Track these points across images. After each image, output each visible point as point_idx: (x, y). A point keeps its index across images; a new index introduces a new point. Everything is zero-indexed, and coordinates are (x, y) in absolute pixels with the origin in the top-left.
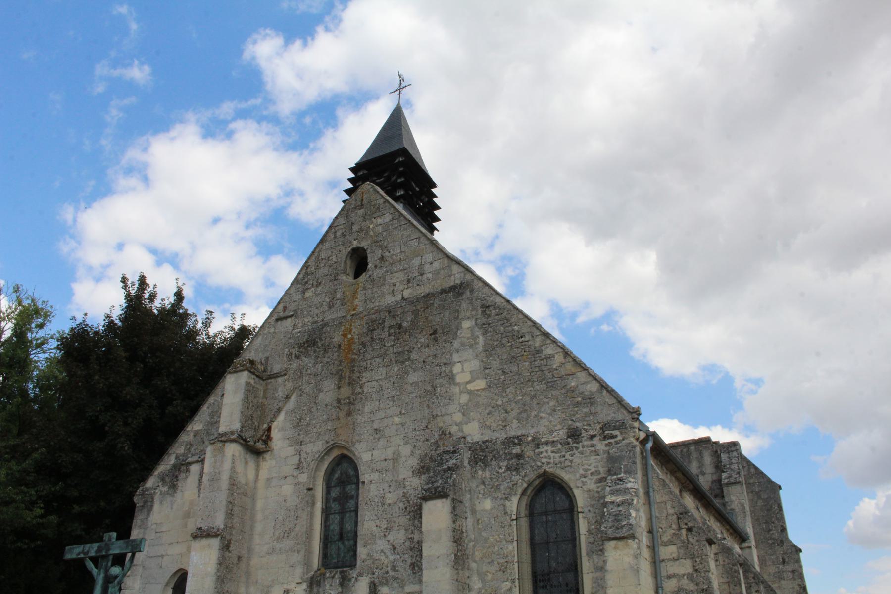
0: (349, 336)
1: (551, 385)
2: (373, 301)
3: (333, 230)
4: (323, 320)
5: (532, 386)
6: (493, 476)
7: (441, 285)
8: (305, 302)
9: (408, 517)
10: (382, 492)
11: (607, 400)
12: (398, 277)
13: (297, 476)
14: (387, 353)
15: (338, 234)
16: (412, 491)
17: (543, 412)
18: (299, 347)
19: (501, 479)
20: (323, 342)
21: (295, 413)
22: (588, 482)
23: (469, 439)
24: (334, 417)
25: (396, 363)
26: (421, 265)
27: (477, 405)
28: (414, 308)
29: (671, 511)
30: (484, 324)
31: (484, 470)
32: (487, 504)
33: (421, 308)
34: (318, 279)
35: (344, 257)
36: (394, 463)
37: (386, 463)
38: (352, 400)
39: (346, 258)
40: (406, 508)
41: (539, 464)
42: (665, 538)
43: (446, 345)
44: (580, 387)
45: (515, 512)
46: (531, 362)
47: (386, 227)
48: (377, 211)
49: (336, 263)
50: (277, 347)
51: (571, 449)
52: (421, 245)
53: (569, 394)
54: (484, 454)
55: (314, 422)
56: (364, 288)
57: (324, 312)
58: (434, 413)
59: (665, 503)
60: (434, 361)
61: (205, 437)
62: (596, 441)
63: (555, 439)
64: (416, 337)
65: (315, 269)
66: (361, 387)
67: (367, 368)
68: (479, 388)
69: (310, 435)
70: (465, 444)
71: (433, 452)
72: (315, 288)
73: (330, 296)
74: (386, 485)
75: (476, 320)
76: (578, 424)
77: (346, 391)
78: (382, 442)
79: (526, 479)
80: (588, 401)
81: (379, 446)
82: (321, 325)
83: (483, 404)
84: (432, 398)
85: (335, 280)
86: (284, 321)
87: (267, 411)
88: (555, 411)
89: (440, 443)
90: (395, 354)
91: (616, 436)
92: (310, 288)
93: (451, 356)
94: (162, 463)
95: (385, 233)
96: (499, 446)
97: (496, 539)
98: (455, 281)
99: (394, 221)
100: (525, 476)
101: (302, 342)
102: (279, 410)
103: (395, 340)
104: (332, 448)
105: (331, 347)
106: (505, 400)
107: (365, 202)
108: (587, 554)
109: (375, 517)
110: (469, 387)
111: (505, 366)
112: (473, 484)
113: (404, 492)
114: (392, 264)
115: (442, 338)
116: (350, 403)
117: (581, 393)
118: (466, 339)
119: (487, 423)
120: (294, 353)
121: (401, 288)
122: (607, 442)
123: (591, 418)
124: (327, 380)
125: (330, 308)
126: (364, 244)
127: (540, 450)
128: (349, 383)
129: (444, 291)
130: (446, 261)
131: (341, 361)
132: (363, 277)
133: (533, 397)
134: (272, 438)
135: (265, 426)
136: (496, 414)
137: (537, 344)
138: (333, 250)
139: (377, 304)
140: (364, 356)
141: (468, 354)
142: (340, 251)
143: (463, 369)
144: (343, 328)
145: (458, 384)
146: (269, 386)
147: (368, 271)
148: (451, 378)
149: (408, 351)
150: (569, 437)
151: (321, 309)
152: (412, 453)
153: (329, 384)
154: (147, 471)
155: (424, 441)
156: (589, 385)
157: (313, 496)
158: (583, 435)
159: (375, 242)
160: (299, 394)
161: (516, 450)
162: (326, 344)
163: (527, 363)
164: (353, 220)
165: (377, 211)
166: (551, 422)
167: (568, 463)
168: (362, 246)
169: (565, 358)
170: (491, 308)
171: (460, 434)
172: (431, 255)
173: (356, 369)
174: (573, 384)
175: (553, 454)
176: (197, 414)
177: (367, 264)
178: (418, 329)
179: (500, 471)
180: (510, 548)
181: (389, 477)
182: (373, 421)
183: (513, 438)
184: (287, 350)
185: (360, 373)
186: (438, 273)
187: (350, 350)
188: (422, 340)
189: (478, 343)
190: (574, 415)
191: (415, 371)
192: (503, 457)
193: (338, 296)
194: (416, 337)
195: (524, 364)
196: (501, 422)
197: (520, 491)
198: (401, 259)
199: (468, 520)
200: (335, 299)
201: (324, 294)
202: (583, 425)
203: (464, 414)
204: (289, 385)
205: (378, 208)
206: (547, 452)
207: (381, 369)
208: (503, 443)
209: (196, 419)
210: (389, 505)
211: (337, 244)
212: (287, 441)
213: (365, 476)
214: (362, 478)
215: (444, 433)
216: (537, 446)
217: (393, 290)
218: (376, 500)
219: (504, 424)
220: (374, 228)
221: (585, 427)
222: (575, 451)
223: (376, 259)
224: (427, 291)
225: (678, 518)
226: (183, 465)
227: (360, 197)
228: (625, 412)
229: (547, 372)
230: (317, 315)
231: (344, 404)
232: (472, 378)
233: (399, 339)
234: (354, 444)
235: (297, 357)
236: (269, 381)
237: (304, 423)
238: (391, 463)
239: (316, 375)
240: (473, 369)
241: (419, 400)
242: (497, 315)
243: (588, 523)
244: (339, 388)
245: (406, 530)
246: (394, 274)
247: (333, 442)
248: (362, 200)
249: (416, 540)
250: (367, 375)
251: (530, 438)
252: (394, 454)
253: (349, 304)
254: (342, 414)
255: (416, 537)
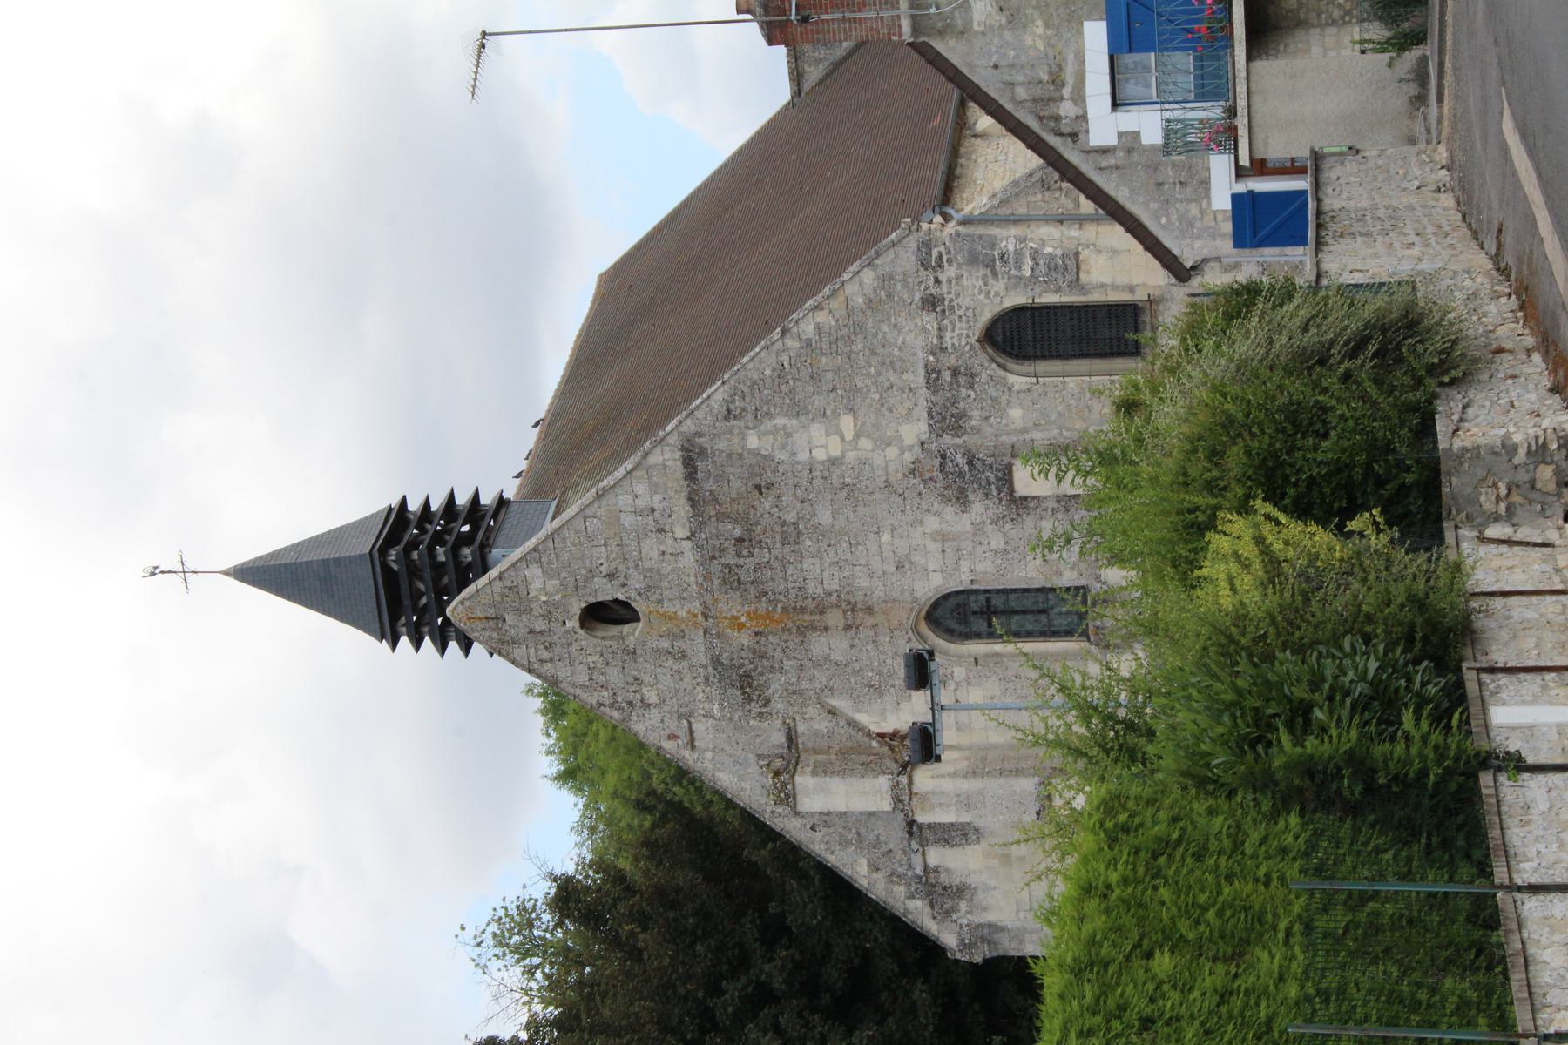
0: (743, 619)
1: (859, 329)
2: (685, 586)
3: (536, 666)
4: (706, 667)
5: (857, 354)
6: (980, 405)
7: (678, 480)
8: (667, 702)
9: (1024, 516)
10: (987, 555)
11: (889, 259)
12: (651, 547)
13: (957, 683)
14: (780, 557)
15: (545, 655)
16: (990, 513)
17: (896, 340)
18: (751, 700)
19: (984, 396)
20: (746, 662)
21: (858, 696)
22: (995, 289)
23: (924, 437)
24: (871, 633)
25: (798, 543)
26: (637, 512)
27: (877, 426)
28: (713, 520)
29: (1039, 196)
30: (756, 417)
31: (970, 418)
32: (1016, 413)
33: (715, 509)
34: (628, 683)
35: (595, 641)
36: (949, 540)
37: (948, 550)
38: (849, 607)
39: (596, 637)
40: (1012, 520)
41: (968, 348)
42: (1071, 206)
43: (781, 471)
44: (865, 292)
45: (1029, 379)
46: (823, 354)
47: (548, 574)
48: (515, 593)
49: (602, 655)
50: (740, 742)
51: (952, 308)
52: (599, 513)
53: (874, 306)
54: (948, 417)
55: (876, 664)
56: (660, 602)
57: (691, 666)
58: (882, 485)
59: (1028, 204)
60: (803, 488)
61: (882, 850)
62: (943, 277)
63: (936, 326)
64: (762, 516)
65: (607, 690)
66: (830, 594)
67: (800, 588)
68: (852, 424)
69: (896, 669)
70: (932, 443)
71: (938, 485)
72: (643, 686)
73: (664, 658)
74: (979, 549)
75: (747, 428)
76: (917, 296)
77: (834, 618)
78: (917, 558)
79: (986, 364)
80: (886, 283)
81: (922, 561)
82: (715, 669)
83: (877, 419)
84: (859, 489)
85: (634, 653)
86: (695, 735)
87: (850, 745)
88: (895, 325)
89: (927, 476)
90: (783, 545)
91: (940, 253)
92: (642, 694)
93: (799, 463)
94: (919, 922)
95: (564, 574)
96: (939, 398)
97: (1061, 403)
98: (675, 460)
99: (543, 560)
100: (982, 365)
101: (741, 697)
102: (852, 723)
103: (761, 548)
104: (918, 634)
105: (757, 647)
106: (873, 389)
107: (491, 613)
108: (1084, 294)
109: (1023, 562)
110: (849, 436)
111: (824, 388)
112: (988, 431)
113: (991, 524)
114: (625, 559)
115: (769, 476)
116: (853, 610)
117: (875, 291)
118: (776, 443)
119: (904, 412)
120: (759, 710)
121: (670, 541)
122: (946, 264)
123: (910, 280)
124: (811, 650)
125: (684, 656)
126: (577, 607)
127: (949, 346)
128: (822, 613)
129: (691, 476)
130: (637, 473)
131: (784, 630)
132: (639, 606)
133: (874, 353)
134: (895, 730)
135: (874, 744)
136: (892, 401)
137: (797, 344)
138: (577, 662)
139: (692, 579)
140: (780, 594)
141: (800, 439)
142: (582, 649)
143: (822, 447)
144: (728, 631)
145: (843, 453)
146: (810, 745)
147: (629, 598)
148: (833, 462)
149: (782, 526)
150: (934, 310)
151: (684, 671)
152: (937, 514)
153: (819, 645)
154: (930, 949)
155: (921, 499)
156: (866, 281)
157: (987, 656)
158: (933, 291)
159: (577, 590)
160: (829, 693)
161: (947, 376)
162: (751, 655)
163: (824, 359)
164: (523, 631)
165: (515, 590)
166: (910, 331)
167: (970, 313)
168: (579, 612)
169: (822, 309)
170: (732, 407)
171: (917, 449)
172: (621, 497)
173: (799, 605)
174: (861, 300)
175: (957, 331)
176: (842, 871)
177: (617, 601)
178: (748, 513)
179: (973, 396)
180: (1072, 385)
181: (967, 545)
182: (884, 573)
183: (929, 379)
184: (751, 723)
185: (806, 598)
186: (656, 485)
187: (768, 616)
188: (767, 506)
189: (785, 425)
190: (904, 301)
191: (815, 515)
192: (955, 393)
193: (665, 644)
194: (762, 516)
195: (824, 363)
196: (905, 395)
197: (1001, 373)
198: (618, 545)
199: (1034, 437)
200: (671, 650)
201: (659, 670)
202: (919, 290)
203: (889, 445)
204: (812, 711)
205: (510, 588)
206: (952, 338)
207: (805, 566)
208: (935, 392)
209: (849, 873)
210: (1006, 543)
211: (567, 656)
212: (902, 704)
213: (961, 581)
214: (966, 585)
215: (912, 471)
216: (943, 349)
217: (672, 554)
218: (999, 561)
219: (907, 391)
220: (546, 594)
221: (922, 288)
222: (955, 303)
223: (609, 586)
224: (683, 501)
225: (1048, 189)
226: (927, 880)
227: (478, 622)
228: (907, 239)
229: (840, 334)
230: (695, 678)
231: (853, 618)
232: (836, 433)
233: (761, 541)
234: (915, 600)
235: (767, 702)
236: (800, 746)
237: (875, 681)
238: (948, 544)
239: (801, 667)
240: (823, 432)
241: (859, 509)
242: (744, 398)
243: (1046, 292)
244: (826, 629)
245: (1041, 519)
246: (643, 555)
247: (910, 632)
248: (487, 618)
249: (1056, 505)
250: (812, 588)
251: (931, 358)
252: (935, 540)
253: (683, 626)
254: (869, 621)
255: (1052, 504)
